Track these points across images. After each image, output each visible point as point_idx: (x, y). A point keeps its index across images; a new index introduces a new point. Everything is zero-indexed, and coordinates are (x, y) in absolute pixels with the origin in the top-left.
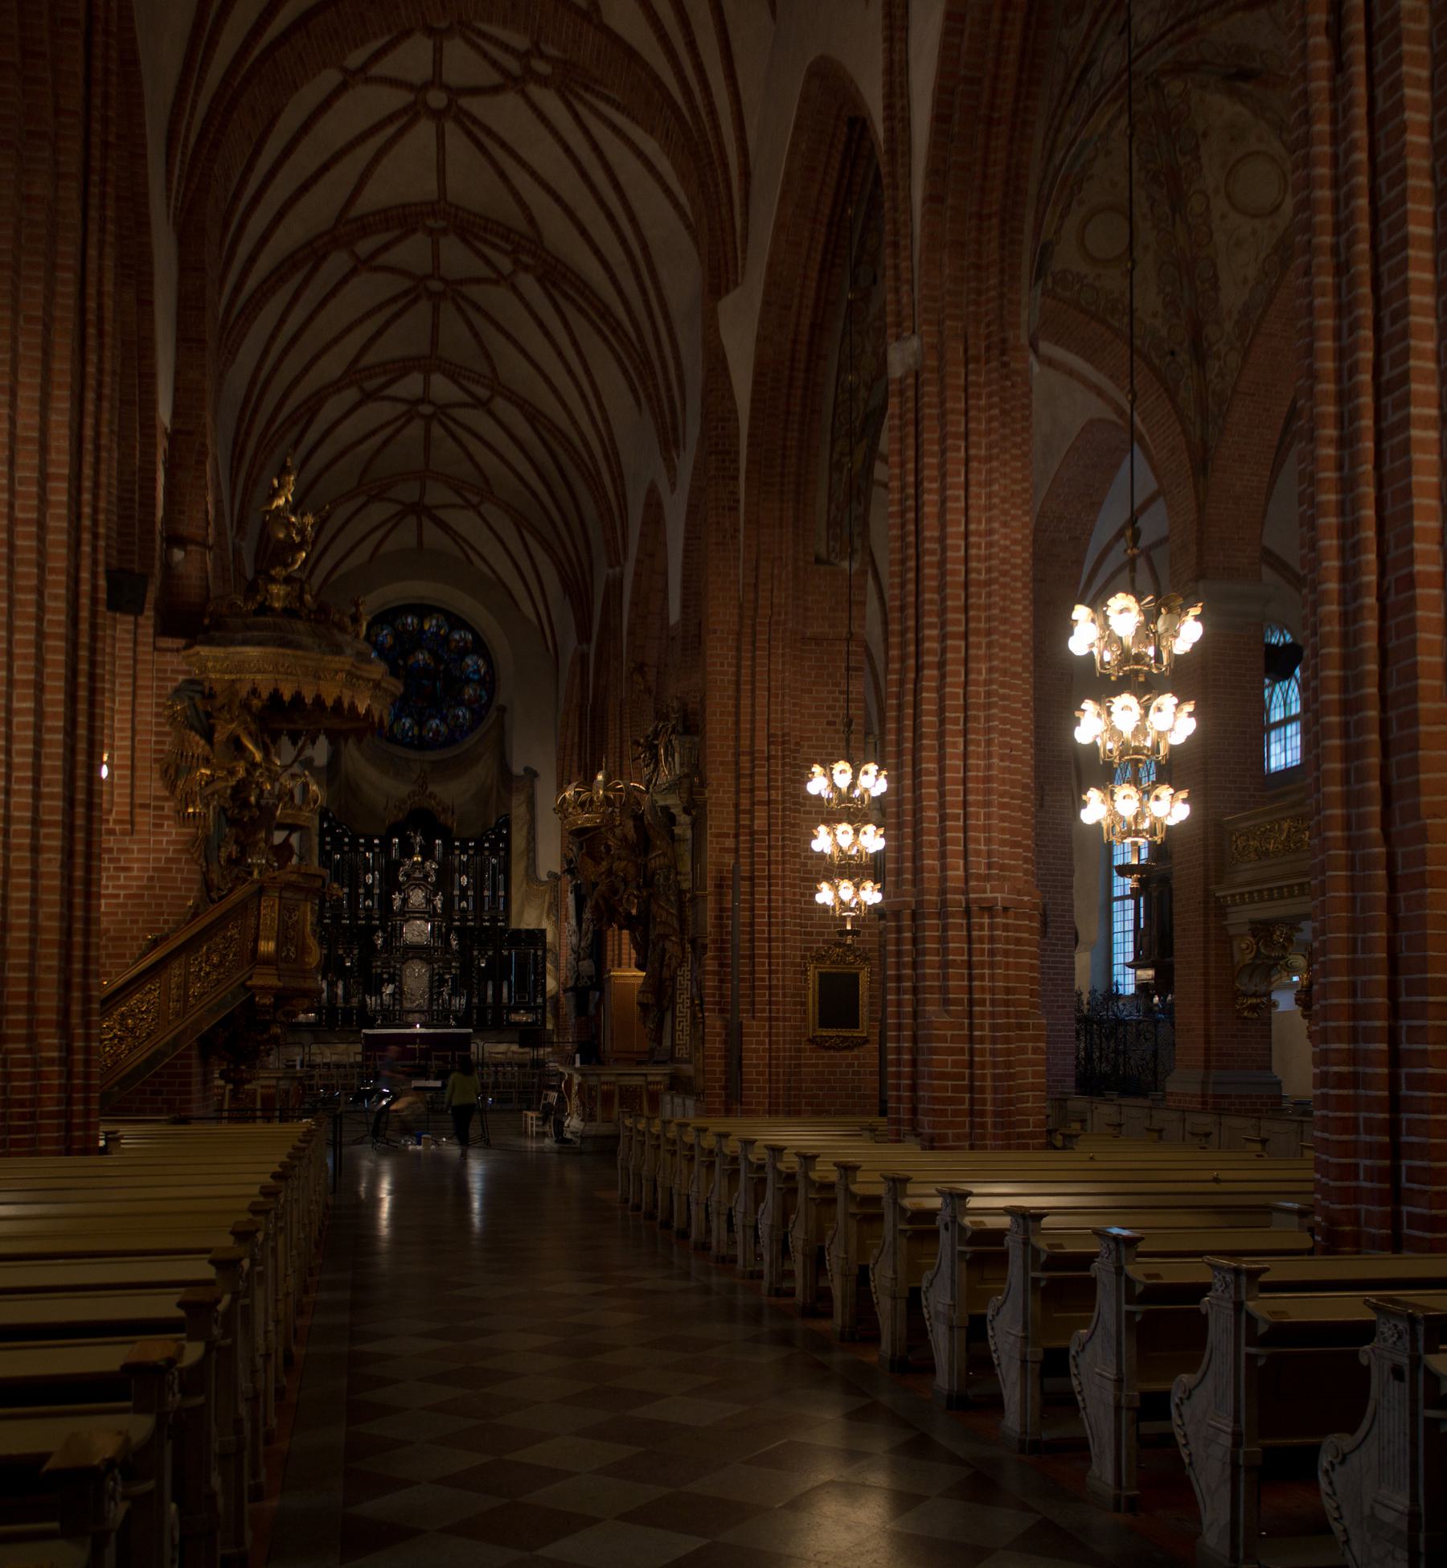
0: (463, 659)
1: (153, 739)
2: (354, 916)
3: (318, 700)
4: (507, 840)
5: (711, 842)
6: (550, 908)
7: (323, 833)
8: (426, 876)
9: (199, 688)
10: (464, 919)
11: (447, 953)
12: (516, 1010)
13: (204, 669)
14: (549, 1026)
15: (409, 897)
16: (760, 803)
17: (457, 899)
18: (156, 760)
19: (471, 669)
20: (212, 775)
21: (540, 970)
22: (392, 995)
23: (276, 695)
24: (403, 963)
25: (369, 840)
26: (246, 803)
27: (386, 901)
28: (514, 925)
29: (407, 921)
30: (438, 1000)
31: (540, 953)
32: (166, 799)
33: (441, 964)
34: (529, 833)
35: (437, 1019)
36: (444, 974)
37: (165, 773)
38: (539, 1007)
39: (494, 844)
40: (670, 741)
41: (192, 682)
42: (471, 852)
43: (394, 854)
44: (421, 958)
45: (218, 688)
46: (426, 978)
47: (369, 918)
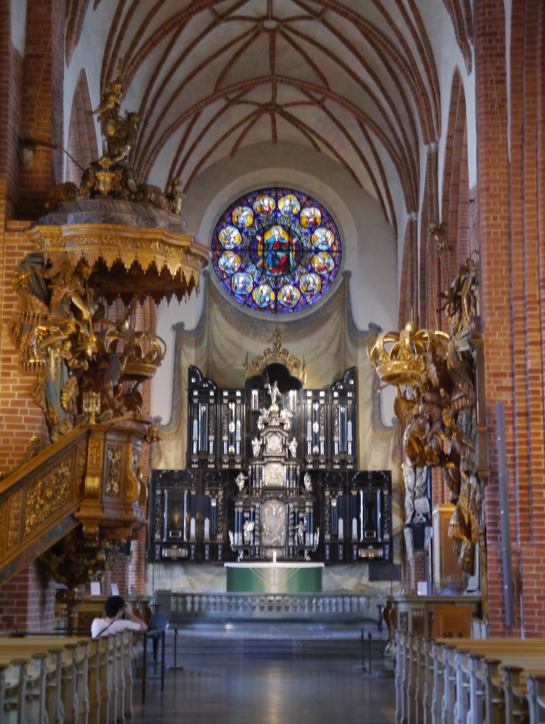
0: (312, 232)
1: (4, 303)
2: (219, 461)
3: (136, 265)
4: (355, 389)
5: (489, 382)
7: (191, 387)
8: (282, 425)
9: (39, 260)
10: (316, 462)
11: (301, 493)
12: (363, 545)
13: (42, 244)
14: (397, 561)
15: (267, 443)
16: (532, 343)
17: (309, 445)
18: (5, 321)
19: (320, 241)
20: (48, 331)
21: (386, 509)
22: (254, 531)
23: (100, 263)
25: (232, 393)
26: (83, 355)
27: (247, 448)
28: (362, 468)
29: (265, 464)
30: (293, 536)
31: (386, 492)
32: (11, 352)
33: (296, 504)
36: (299, 512)
37: (12, 330)
39: (343, 394)
40: (472, 292)
41: (32, 255)
43: (254, 405)
44: (278, 499)
45: (54, 259)
46: (283, 516)
47: (232, 462)
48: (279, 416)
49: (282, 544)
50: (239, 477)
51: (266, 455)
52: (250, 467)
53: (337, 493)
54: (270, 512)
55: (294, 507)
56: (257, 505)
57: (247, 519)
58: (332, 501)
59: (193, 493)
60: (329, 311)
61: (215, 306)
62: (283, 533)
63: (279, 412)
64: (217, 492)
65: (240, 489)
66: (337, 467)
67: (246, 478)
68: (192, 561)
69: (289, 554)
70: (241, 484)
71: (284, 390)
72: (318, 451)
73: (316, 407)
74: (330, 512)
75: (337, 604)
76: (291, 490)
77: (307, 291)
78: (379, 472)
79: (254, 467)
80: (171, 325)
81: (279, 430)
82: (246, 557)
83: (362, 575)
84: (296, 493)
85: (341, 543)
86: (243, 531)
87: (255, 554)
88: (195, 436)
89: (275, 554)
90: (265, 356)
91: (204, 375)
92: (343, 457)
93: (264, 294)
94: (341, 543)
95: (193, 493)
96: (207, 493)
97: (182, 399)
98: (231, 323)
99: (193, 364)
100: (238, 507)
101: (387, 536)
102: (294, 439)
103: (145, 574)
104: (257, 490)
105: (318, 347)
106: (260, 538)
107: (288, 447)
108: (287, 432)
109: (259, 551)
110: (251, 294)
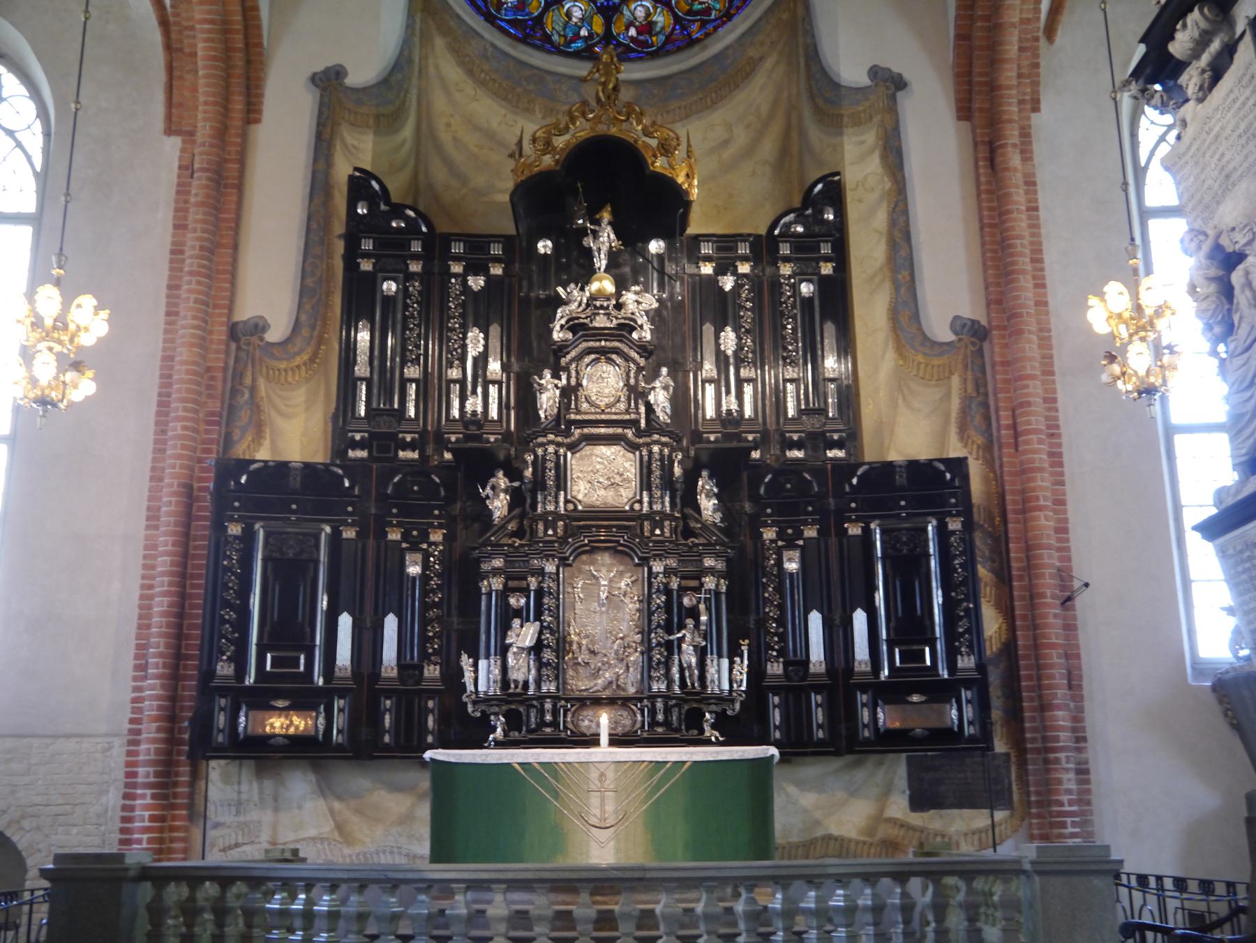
6: (964, 412)
7: (355, 230)
8: (628, 327)
11: (688, 533)
12: (892, 693)
14: (1000, 746)
15: (579, 385)
22: (537, 648)
24: (564, 562)
28: (870, 454)
29: (573, 447)
30: (668, 666)
31: (954, 525)
33: (672, 563)
34: (892, 223)
35: (667, 723)
36: (683, 590)
38: (968, 683)
42: (744, 268)
44: (615, 551)
46: (631, 606)
48: (619, 306)
49: (632, 690)
50: (493, 480)
51: (579, 417)
52: (530, 458)
53: (799, 534)
54: (591, 593)
55: (668, 572)
56: (550, 568)
57: (518, 613)
58: (786, 554)
59: (349, 534)
60: (752, 52)
61: (439, 42)
63: (618, 294)
64: (424, 536)
65: (497, 514)
66: (798, 454)
67: (516, 484)
68: (340, 748)
69: (654, 723)
70: (499, 505)
71: (632, 237)
72: (734, 407)
73: (728, 283)
74: (779, 589)
75: (878, 909)
76: (655, 519)
77: (690, 12)
78: (931, 461)
79: (540, 451)
80: (309, 74)
81: (616, 344)
82: (515, 735)
83: (887, 791)
84: (674, 531)
86: (504, 650)
87: (542, 724)
88: (361, 369)
89: (604, 721)
90: (573, 120)
91: (395, 198)
92: (812, 424)
93: (574, 20)
94: (818, 689)
95: (349, 534)
96: (395, 535)
97: (330, 269)
98: (482, 84)
99: (368, 167)
100: (485, 576)
101: (966, 662)
102: (664, 370)
103: (191, 796)
104: (551, 520)
105: (726, 143)
106: (559, 674)
108: (644, 349)
109: (555, 712)
110: (539, 21)
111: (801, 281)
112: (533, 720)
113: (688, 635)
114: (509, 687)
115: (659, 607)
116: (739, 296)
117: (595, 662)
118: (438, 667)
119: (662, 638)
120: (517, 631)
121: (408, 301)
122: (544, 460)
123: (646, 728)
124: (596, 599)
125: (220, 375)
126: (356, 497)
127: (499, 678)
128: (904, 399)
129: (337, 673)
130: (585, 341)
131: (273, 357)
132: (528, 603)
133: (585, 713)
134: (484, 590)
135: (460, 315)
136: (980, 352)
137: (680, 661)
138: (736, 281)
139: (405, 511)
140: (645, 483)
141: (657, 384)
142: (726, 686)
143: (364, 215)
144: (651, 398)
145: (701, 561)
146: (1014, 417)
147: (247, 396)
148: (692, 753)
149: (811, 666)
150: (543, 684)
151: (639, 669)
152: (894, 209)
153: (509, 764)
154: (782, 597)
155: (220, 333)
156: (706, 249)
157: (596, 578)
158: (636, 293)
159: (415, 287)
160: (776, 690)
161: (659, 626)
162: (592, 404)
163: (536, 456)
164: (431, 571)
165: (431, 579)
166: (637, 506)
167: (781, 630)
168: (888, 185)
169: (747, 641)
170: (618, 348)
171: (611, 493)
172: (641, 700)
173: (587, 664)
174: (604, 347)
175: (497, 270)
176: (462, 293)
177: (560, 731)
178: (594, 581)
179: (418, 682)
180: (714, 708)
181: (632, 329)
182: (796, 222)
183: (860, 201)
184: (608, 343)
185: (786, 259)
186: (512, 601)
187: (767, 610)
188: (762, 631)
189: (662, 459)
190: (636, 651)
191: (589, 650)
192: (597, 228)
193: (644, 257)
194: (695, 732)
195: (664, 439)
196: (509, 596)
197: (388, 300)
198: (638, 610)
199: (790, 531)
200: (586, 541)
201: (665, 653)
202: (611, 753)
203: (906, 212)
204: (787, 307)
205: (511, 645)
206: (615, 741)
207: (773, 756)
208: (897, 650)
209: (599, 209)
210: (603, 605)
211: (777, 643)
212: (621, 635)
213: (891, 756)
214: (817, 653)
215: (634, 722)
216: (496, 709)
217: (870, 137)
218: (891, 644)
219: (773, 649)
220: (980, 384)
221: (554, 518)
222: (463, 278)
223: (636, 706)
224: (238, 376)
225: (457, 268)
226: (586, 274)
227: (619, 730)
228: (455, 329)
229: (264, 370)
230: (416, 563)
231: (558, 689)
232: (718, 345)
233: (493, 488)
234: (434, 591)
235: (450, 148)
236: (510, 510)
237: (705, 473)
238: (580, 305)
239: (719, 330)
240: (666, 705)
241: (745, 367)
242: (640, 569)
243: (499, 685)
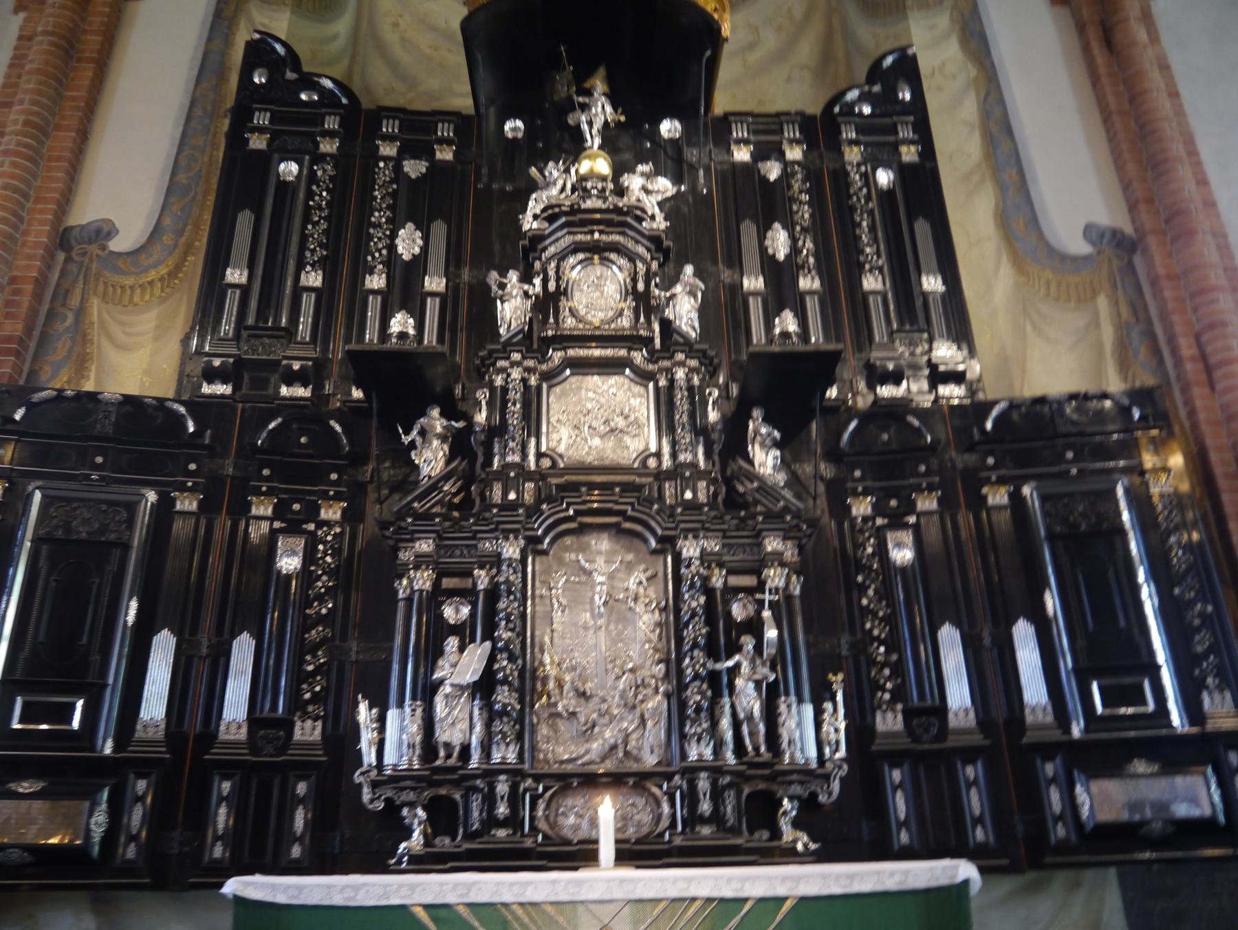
7: (249, 98)
15: (562, 292)
17: (756, 309)
22: (484, 687)
24: (533, 545)
29: (550, 377)
33: (714, 546)
44: (618, 531)
46: (646, 621)
48: (621, 191)
49: (650, 761)
53: (910, 508)
57: (456, 630)
58: (891, 537)
59: (187, 503)
62: (656, 703)
64: (312, 512)
67: (460, 425)
68: (128, 869)
69: (692, 820)
74: (885, 593)
79: (499, 381)
81: (616, 238)
82: (444, 843)
85: (969, 755)
86: (427, 691)
95: (187, 503)
96: (263, 508)
102: (689, 269)
105: (751, 46)
107: (659, 309)
108: (655, 240)
109: (514, 799)
111: (874, 170)
112: (476, 814)
113: (745, 668)
114: (436, 757)
115: (694, 615)
116: (790, 187)
117: (587, 712)
118: (319, 724)
119: (704, 665)
120: (453, 658)
121: (314, 188)
122: (505, 390)
123: (680, 828)
124: (588, 607)
125: (29, 288)
126: (205, 447)
127: (418, 739)
128: (1034, 326)
129: (139, 733)
130: (569, 233)
131: (117, 270)
132: (473, 614)
133: (569, 802)
134: (401, 595)
135: (388, 207)
136: (1131, 266)
137: (733, 706)
138: (784, 170)
139: (282, 473)
140: (666, 423)
141: (678, 289)
142: (812, 752)
143: (261, 85)
144: (669, 313)
145: (760, 545)
146: (1199, 345)
147: (70, 319)
148: (797, 879)
149: (951, 716)
150: (494, 747)
151: (663, 723)
152: (986, 99)
153: (403, 907)
154: (892, 604)
155: (39, 233)
156: (738, 132)
157: (589, 573)
158: (642, 174)
159: (323, 172)
160: (895, 757)
161: (695, 645)
162: (580, 320)
163: (492, 389)
164: (318, 565)
165: (319, 578)
166: (652, 463)
167: (894, 657)
168: (973, 71)
169: (840, 677)
170: (618, 243)
171: (611, 444)
172: (669, 777)
173: (573, 714)
174: (598, 241)
175: (445, 154)
176: (392, 181)
177: (523, 835)
178: (584, 578)
179: (282, 750)
180: (797, 789)
181: (640, 220)
182: (863, 98)
183: (939, 88)
184: (604, 237)
185: (852, 142)
186: (449, 612)
187: (868, 626)
188: (862, 658)
189: (690, 389)
190: (656, 690)
191: (577, 690)
192: (587, 100)
193: (652, 142)
194: (766, 834)
195: (693, 363)
196: (442, 603)
197: (284, 187)
198: (659, 624)
199: (893, 503)
200: (571, 512)
201: (709, 693)
202: (623, 881)
203: (1001, 101)
204: (859, 199)
205: (441, 682)
206: (629, 854)
207: (966, 883)
208: (1095, 687)
209: (590, 73)
210: (600, 615)
211: (889, 678)
212: (630, 665)
213: (1090, 874)
214: (958, 694)
215: (658, 819)
216: (411, 796)
217: (943, 21)
218: (1083, 677)
219: (884, 690)
220: (1138, 307)
221: (517, 476)
222: (397, 162)
223: (661, 787)
224: (62, 294)
225: (388, 150)
226: (574, 147)
227: (631, 832)
228: (379, 225)
229: (101, 287)
230: (294, 553)
231: (520, 756)
232: (763, 249)
233: (423, 433)
234: (321, 598)
235: (397, 50)
236: (448, 462)
237: (757, 413)
238: (563, 189)
239: (764, 228)
240: (714, 784)
241: (805, 276)
242: (661, 558)
243: (418, 752)
